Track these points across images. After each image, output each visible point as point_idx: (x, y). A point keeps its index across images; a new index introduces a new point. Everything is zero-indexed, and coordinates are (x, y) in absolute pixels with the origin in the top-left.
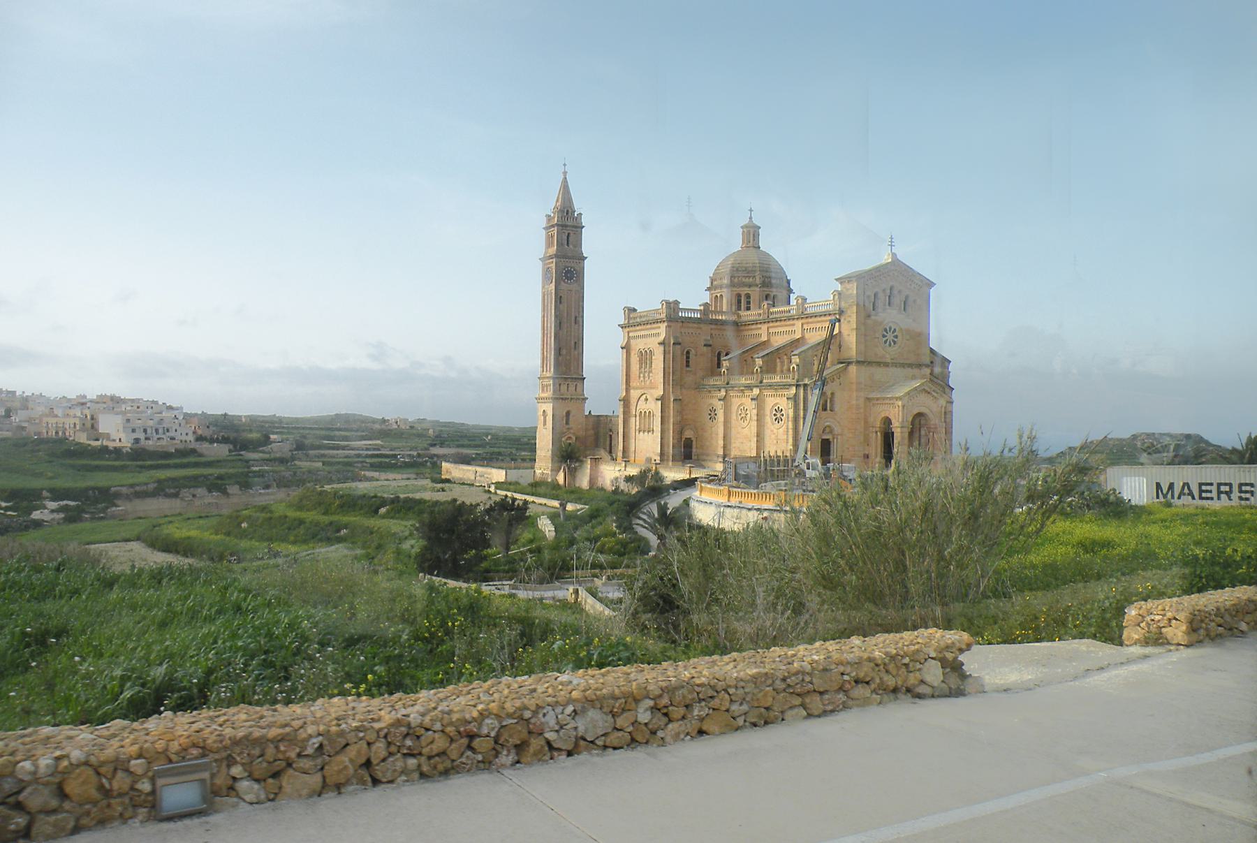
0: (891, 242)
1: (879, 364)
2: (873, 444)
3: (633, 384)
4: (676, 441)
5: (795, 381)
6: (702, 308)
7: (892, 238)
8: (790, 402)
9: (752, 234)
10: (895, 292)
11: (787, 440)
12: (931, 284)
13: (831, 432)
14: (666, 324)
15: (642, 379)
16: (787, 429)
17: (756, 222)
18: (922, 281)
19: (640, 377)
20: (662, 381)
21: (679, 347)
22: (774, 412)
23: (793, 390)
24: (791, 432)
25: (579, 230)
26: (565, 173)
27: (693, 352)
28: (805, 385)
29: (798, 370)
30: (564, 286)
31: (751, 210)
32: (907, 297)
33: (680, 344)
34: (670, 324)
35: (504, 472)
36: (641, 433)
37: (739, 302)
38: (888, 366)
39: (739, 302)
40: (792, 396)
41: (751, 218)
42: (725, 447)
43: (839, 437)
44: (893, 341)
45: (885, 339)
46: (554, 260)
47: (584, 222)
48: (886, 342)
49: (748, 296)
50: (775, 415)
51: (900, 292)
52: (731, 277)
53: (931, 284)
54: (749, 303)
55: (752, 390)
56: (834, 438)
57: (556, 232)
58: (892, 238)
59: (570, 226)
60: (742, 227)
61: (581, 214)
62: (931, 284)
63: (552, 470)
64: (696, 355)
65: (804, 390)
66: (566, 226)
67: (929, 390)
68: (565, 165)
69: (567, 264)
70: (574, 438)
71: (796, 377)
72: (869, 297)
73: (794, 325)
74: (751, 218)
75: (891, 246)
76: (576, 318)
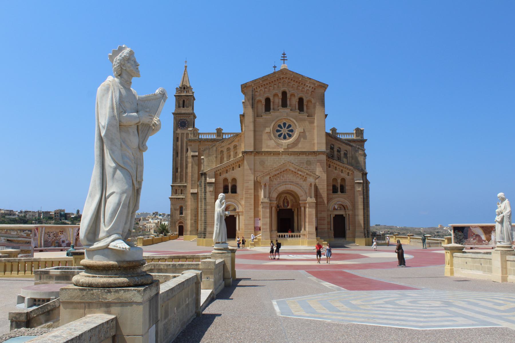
0: (284, 57)
4: (193, 221)
7: (284, 54)
10: (288, 95)
12: (324, 87)
13: (235, 209)
21: (196, 158)
25: (189, 97)
26: (186, 67)
30: (179, 131)
44: (288, 134)
45: (279, 133)
48: (280, 136)
51: (293, 95)
53: (324, 87)
58: (284, 54)
59: (184, 96)
66: (181, 96)
67: (293, 170)
68: (186, 62)
69: (181, 118)
72: (260, 101)
75: (284, 60)
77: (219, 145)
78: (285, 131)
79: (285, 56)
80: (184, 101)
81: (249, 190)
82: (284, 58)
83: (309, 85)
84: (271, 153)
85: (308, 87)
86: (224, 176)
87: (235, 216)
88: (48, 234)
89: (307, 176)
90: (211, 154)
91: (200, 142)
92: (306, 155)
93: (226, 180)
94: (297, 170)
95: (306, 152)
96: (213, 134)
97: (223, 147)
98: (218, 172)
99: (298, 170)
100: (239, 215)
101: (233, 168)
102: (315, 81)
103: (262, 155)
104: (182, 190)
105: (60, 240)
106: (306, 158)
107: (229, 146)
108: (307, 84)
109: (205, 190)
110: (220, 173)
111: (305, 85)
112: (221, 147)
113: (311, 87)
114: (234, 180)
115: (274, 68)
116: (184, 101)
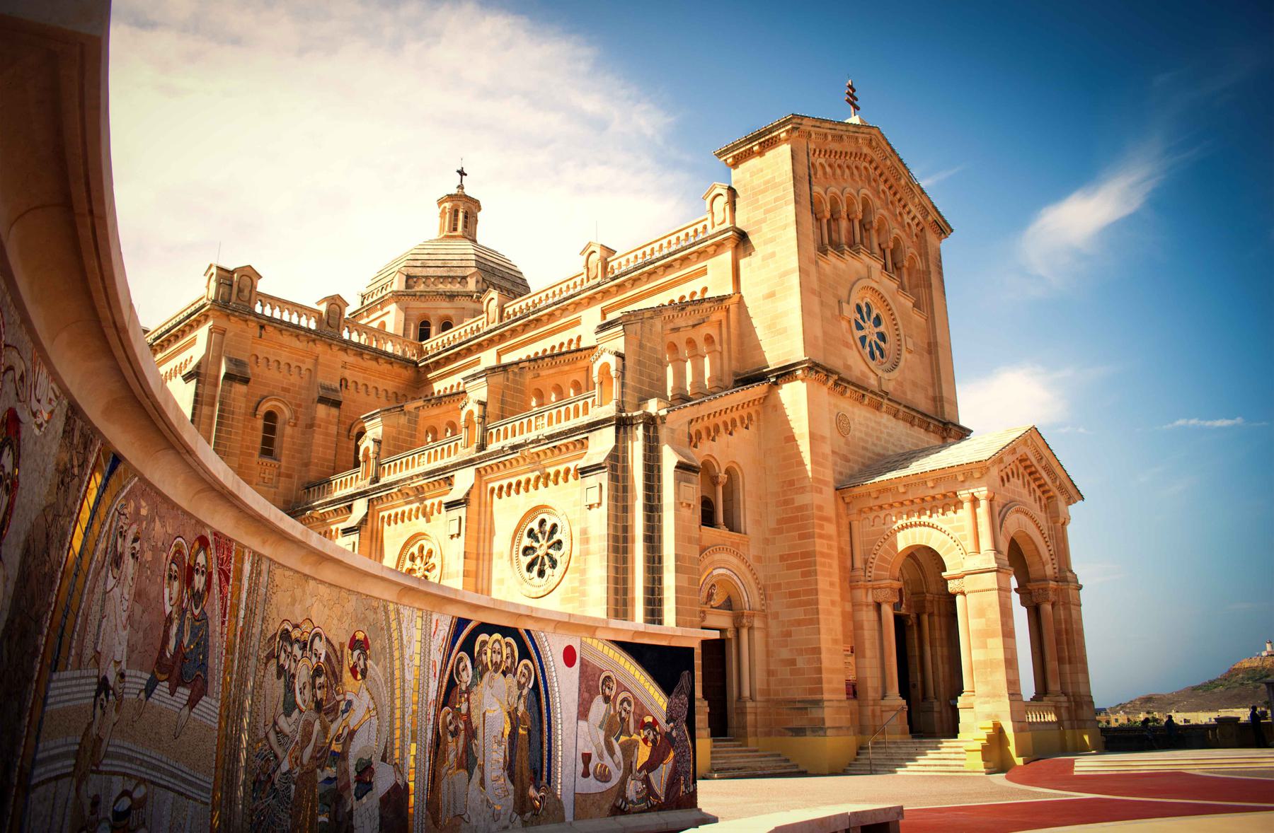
0: (851, 95)
2: (868, 653)
6: (323, 308)
18: (925, 213)
21: (239, 388)
22: (526, 542)
27: (285, 413)
28: (651, 423)
31: (462, 173)
32: (897, 241)
33: (246, 381)
34: (224, 323)
41: (461, 187)
43: (757, 623)
50: (527, 550)
52: (409, 277)
53: (943, 229)
55: (449, 481)
60: (440, 202)
64: (295, 425)
65: (647, 438)
74: (461, 187)
77: (671, 317)
78: (870, 330)
79: (855, 94)
81: (825, 524)
82: (852, 101)
83: (914, 211)
84: (863, 395)
85: (912, 215)
88: (281, 670)
89: (1057, 493)
90: (648, 345)
91: (262, 327)
94: (1044, 463)
95: (932, 421)
97: (676, 330)
99: (1044, 468)
100: (751, 629)
102: (930, 206)
103: (842, 394)
105: (342, 756)
107: (692, 334)
110: (698, 434)
111: (904, 206)
112: (671, 326)
113: (916, 221)
115: (458, 176)
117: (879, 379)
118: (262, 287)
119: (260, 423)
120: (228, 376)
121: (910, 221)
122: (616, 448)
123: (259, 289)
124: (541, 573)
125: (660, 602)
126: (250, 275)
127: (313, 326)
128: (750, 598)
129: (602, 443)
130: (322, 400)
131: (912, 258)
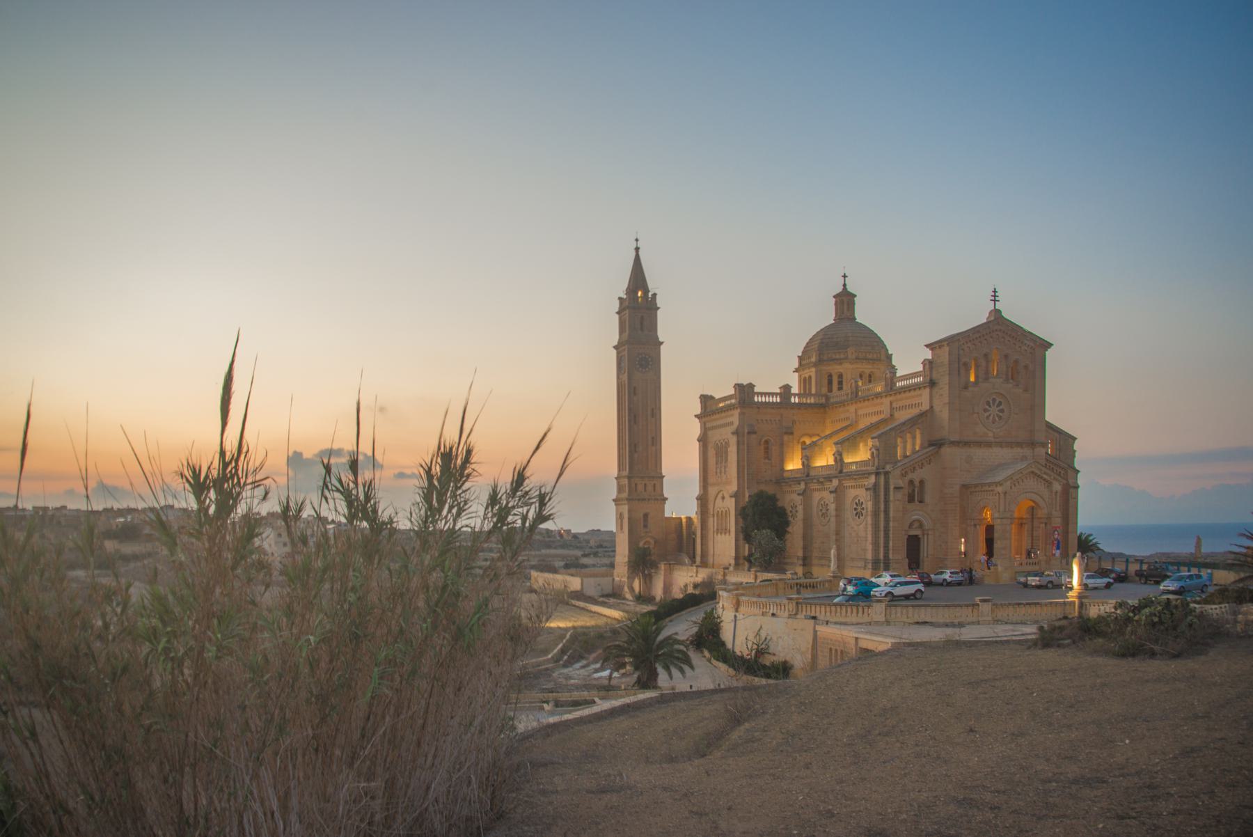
1: (979, 444)
3: (711, 480)
5: (874, 468)
8: (868, 492)
9: (845, 301)
11: (866, 537)
12: (1048, 345)
13: (921, 526)
14: (739, 410)
15: (719, 474)
16: (866, 524)
17: (849, 289)
19: (716, 473)
20: (736, 475)
21: (754, 436)
22: (855, 506)
23: (872, 479)
24: (870, 528)
26: (637, 249)
28: (887, 473)
29: (878, 456)
31: (845, 276)
32: (1016, 362)
33: (755, 433)
35: (580, 581)
36: (719, 534)
37: (830, 382)
38: (990, 446)
39: (830, 382)
40: (870, 486)
41: (845, 285)
42: (805, 548)
46: (626, 346)
47: (659, 302)
49: (840, 376)
50: (855, 509)
54: (840, 383)
55: (831, 481)
56: (923, 535)
57: (627, 315)
60: (834, 297)
61: (654, 295)
62: (1048, 345)
63: (628, 578)
65: (885, 478)
67: (1039, 473)
68: (637, 240)
70: (652, 542)
71: (876, 464)
73: (882, 404)
74: (845, 285)
76: (653, 410)
78: (994, 410)
80: (642, 318)
86: (910, 476)
87: (920, 536)
92: (1022, 447)
93: (911, 482)
96: (776, 394)
98: (903, 472)
99: (1045, 473)
101: (922, 464)
104: (645, 485)
106: (1022, 451)
108: (1026, 342)
109: (885, 498)
114: (922, 482)
115: (843, 278)
116: (642, 318)
117: (994, 433)
118: (756, 390)
119: (762, 447)
120: (749, 433)
121: (1026, 348)
122: (875, 483)
123: (755, 391)
124: (859, 517)
125: (889, 530)
126: (751, 386)
127: (778, 400)
128: (927, 524)
129: (872, 479)
130: (786, 433)
131: (1026, 367)
